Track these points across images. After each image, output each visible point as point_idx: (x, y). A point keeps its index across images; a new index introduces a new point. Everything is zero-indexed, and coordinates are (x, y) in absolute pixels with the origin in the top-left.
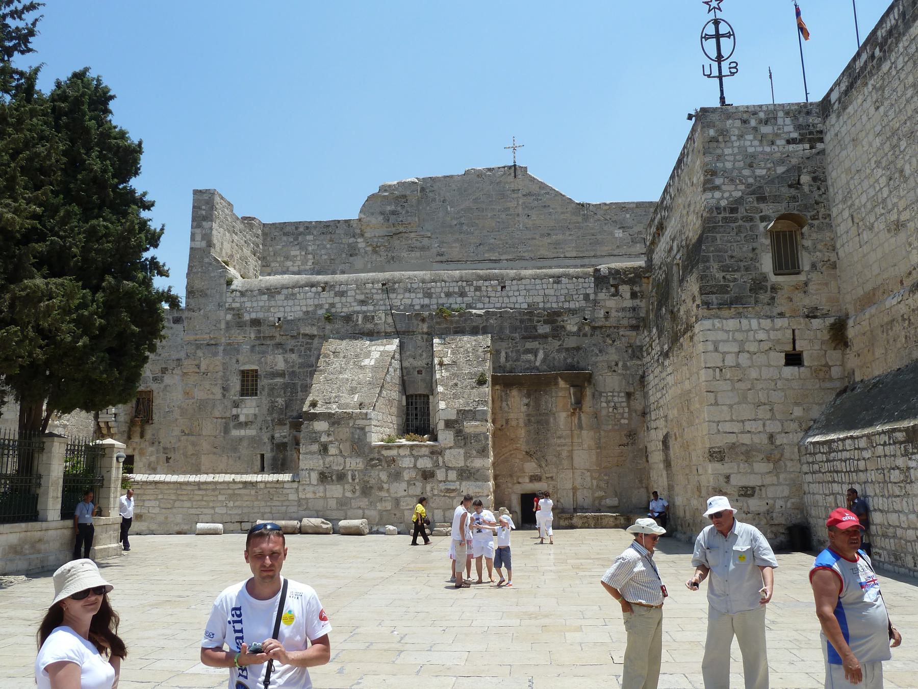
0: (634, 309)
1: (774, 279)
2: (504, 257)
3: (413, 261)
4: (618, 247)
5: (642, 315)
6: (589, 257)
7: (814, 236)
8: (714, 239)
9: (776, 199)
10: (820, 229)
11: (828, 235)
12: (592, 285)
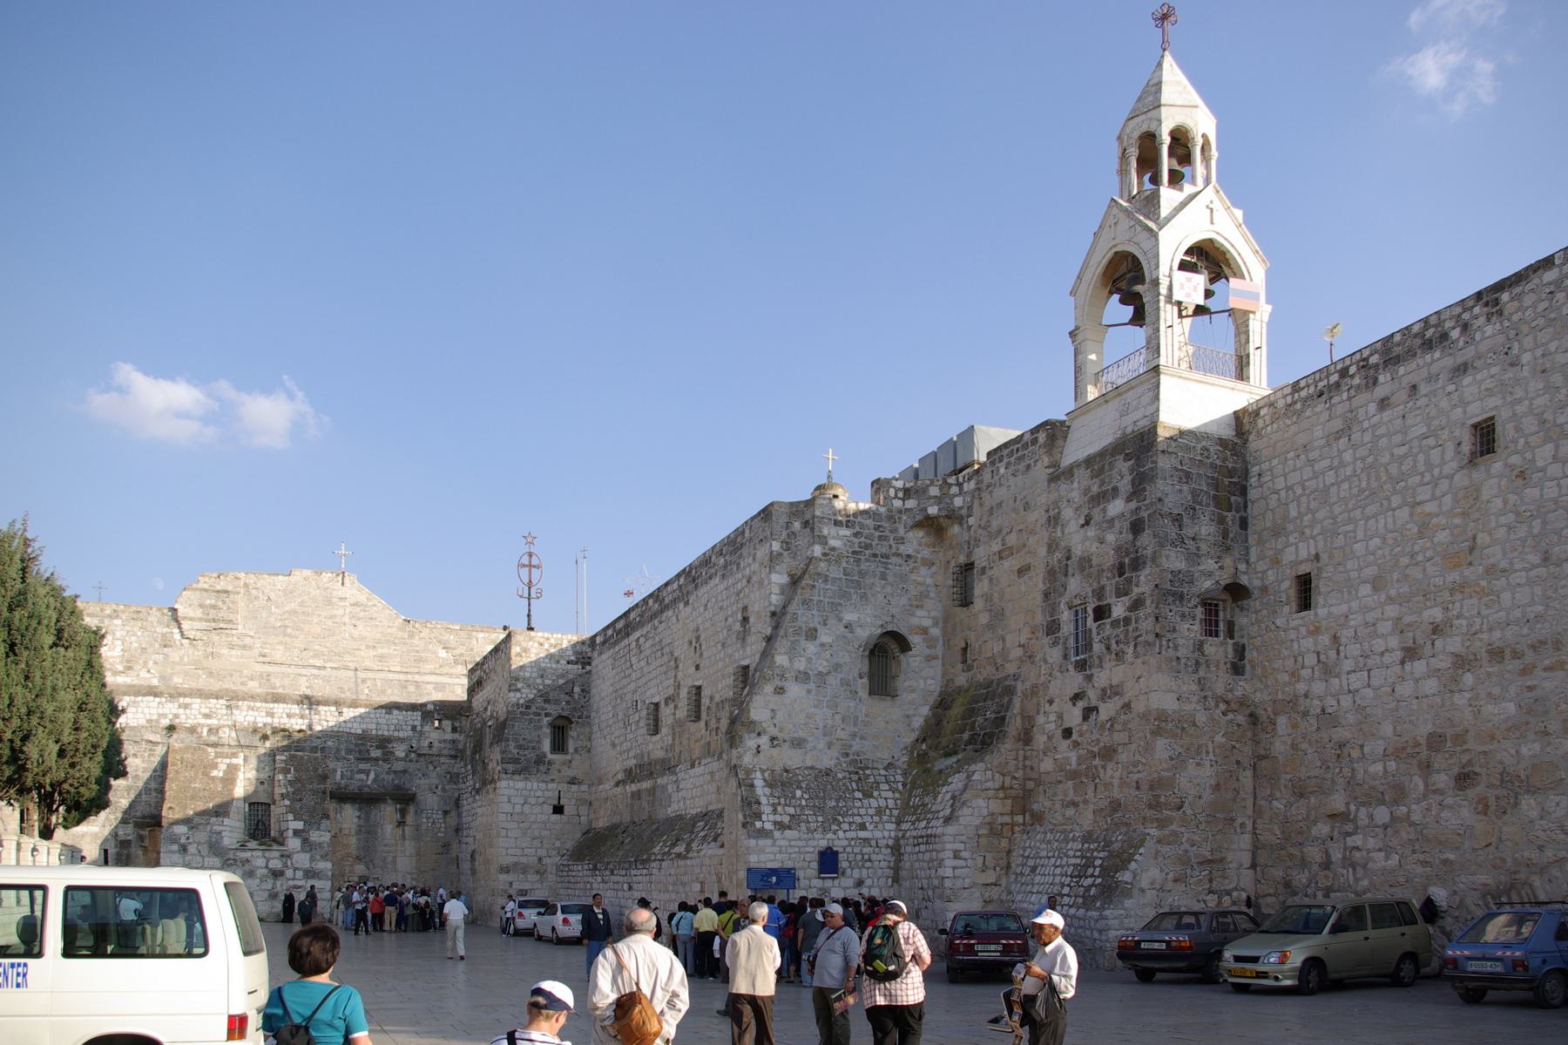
0: (454, 742)
1: (550, 756)
2: (328, 665)
3: (234, 660)
4: (441, 666)
5: (460, 747)
6: (412, 673)
7: (579, 730)
8: (513, 726)
9: (557, 702)
10: (583, 725)
11: (588, 730)
12: (419, 718)
